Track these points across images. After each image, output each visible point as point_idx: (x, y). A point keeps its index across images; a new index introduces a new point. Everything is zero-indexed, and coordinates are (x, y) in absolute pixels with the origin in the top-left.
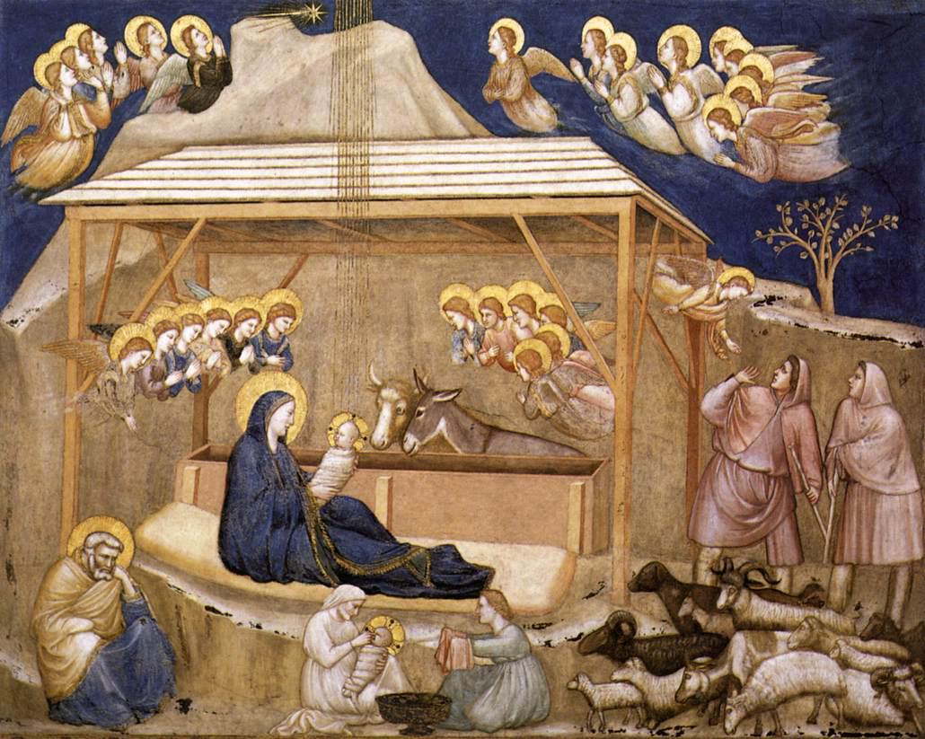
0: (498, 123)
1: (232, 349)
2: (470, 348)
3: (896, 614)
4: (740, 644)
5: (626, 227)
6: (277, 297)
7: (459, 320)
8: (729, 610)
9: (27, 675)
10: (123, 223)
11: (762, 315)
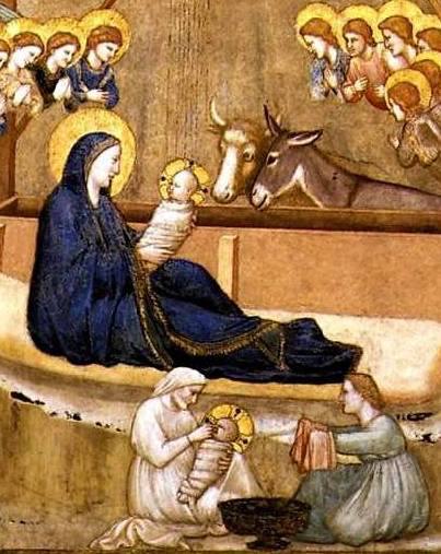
1: (44, 82)
2: (333, 80)
6: (99, 19)
7: (319, 46)
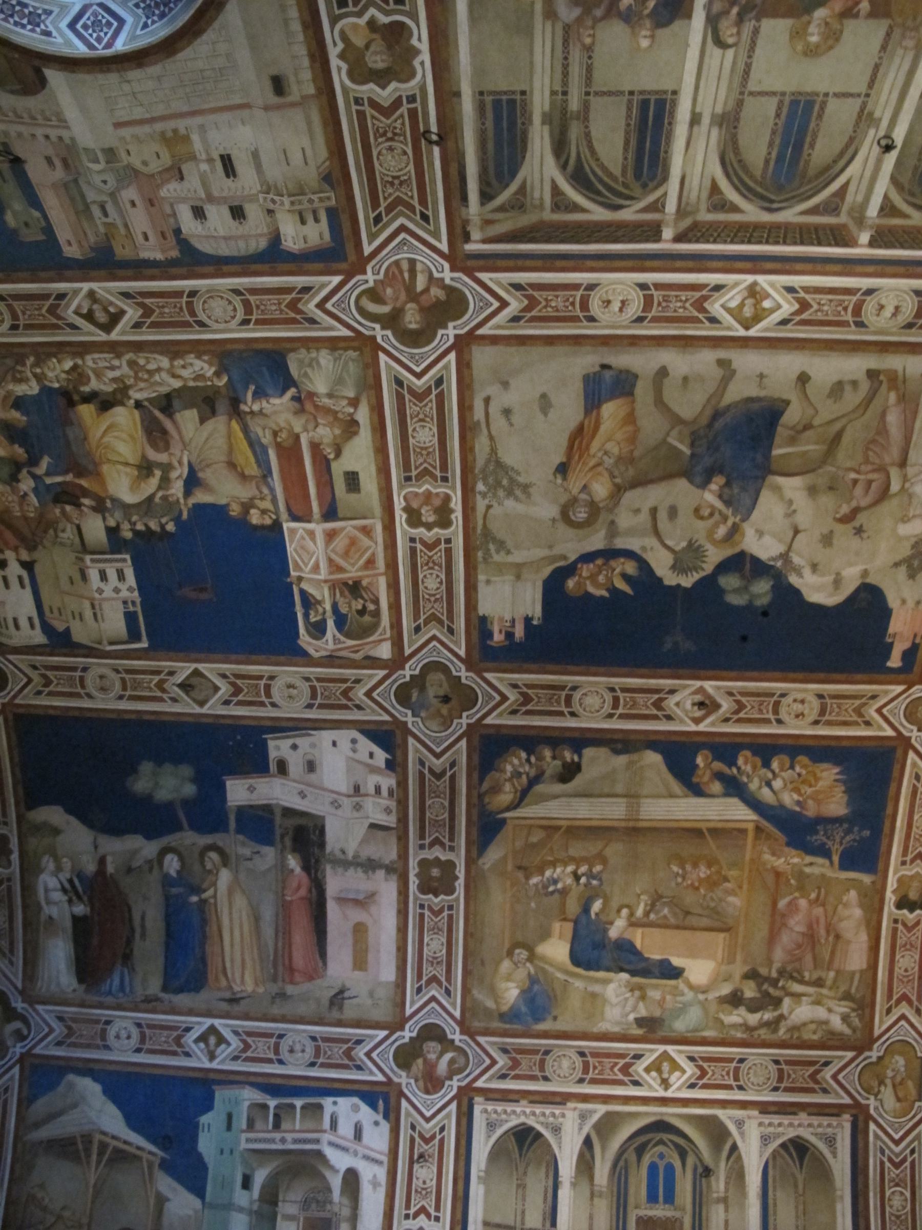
0: (698, 791)
2: (679, 880)
3: (853, 991)
4: (787, 1001)
5: (751, 835)
8: (783, 988)
9: (490, 1004)
10: (531, 826)
11: (807, 870)
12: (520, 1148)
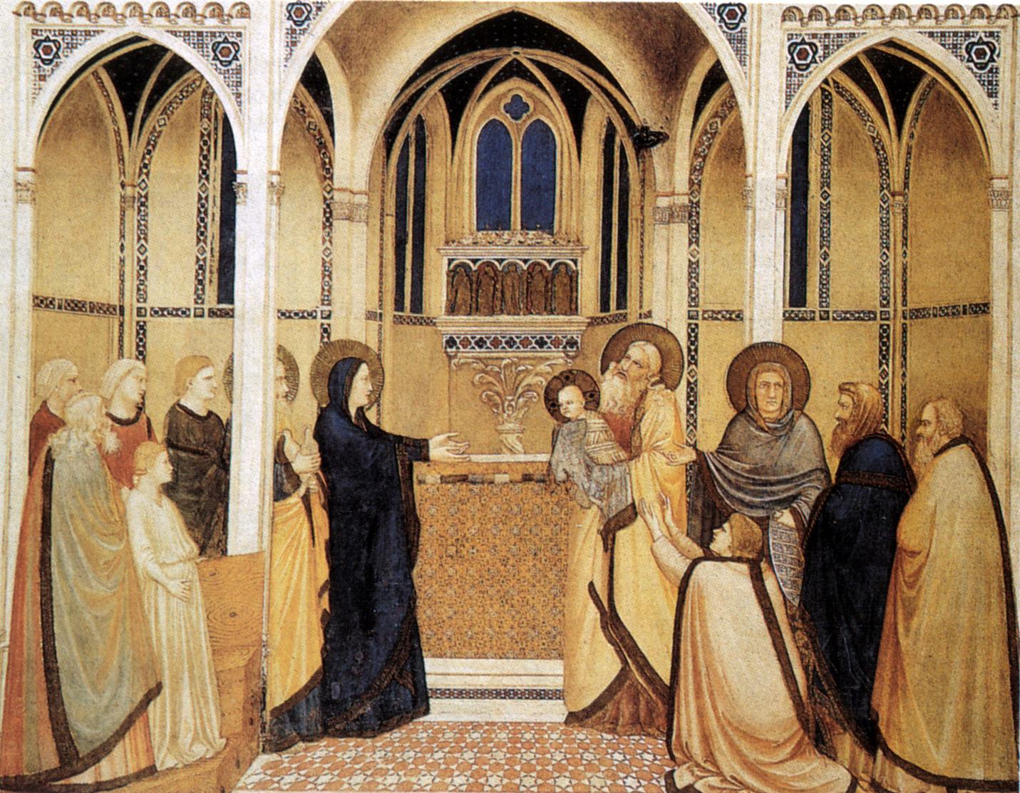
12: (129, 105)
